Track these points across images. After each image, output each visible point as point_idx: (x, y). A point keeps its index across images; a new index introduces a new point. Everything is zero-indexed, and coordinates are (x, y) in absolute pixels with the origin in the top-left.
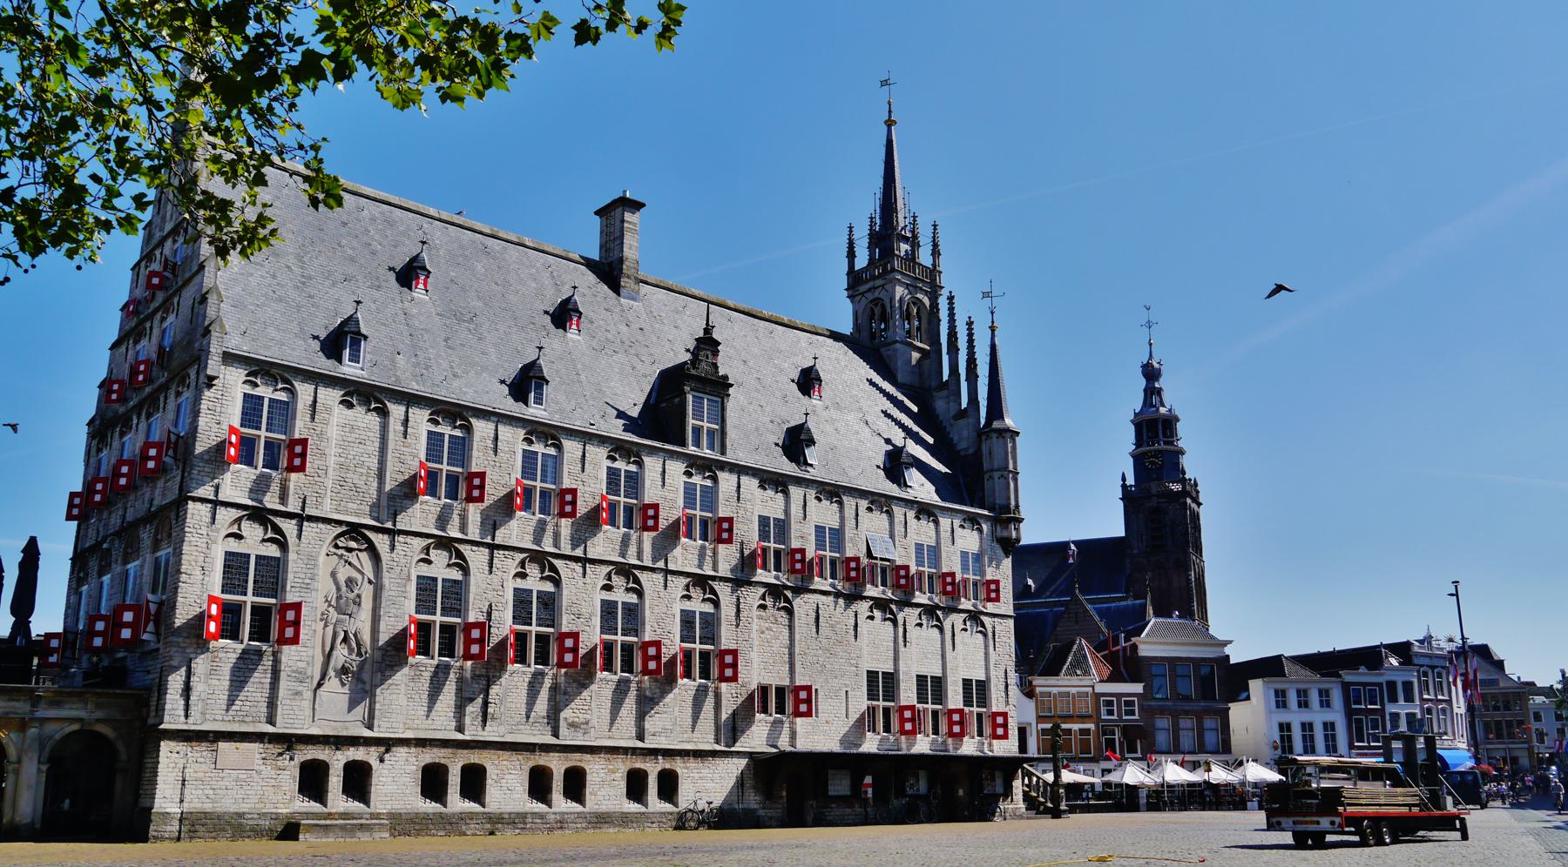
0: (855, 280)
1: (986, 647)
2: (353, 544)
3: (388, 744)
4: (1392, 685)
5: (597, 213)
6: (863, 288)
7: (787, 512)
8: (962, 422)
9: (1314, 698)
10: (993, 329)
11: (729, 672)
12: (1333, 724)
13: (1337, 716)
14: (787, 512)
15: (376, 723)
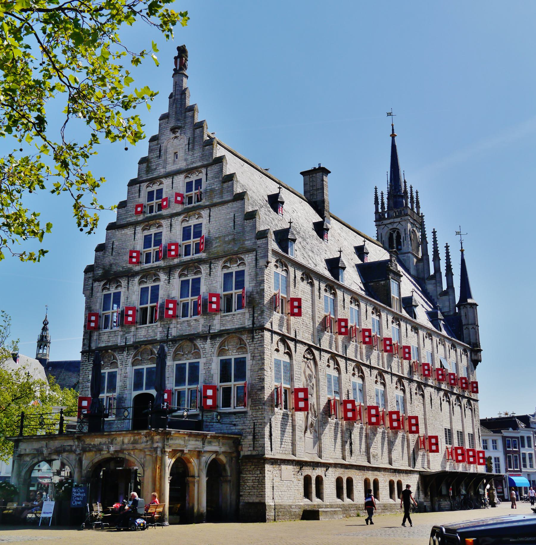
0: (379, 218)
1: (472, 416)
2: (309, 356)
3: (327, 466)
4: (522, 438)
5: (302, 173)
6: (385, 222)
7: (418, 344)
8: (445, 298)
9: (490, 445)
10: (462, 251)
11: (414, 428)
12: (498, 458)
13: (499, 454)
14: (418, 344)
15: (323, 454)
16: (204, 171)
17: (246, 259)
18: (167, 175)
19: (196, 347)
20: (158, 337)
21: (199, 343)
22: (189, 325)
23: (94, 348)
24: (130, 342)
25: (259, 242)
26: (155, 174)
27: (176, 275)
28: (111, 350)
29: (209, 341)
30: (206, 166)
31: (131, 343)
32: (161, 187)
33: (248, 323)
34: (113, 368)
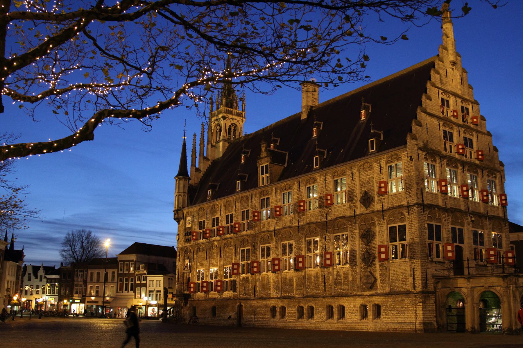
16: (471, 104)
24: (449, 207)
25: (501, 168)
30: (472, 103)
32: (448, 99)
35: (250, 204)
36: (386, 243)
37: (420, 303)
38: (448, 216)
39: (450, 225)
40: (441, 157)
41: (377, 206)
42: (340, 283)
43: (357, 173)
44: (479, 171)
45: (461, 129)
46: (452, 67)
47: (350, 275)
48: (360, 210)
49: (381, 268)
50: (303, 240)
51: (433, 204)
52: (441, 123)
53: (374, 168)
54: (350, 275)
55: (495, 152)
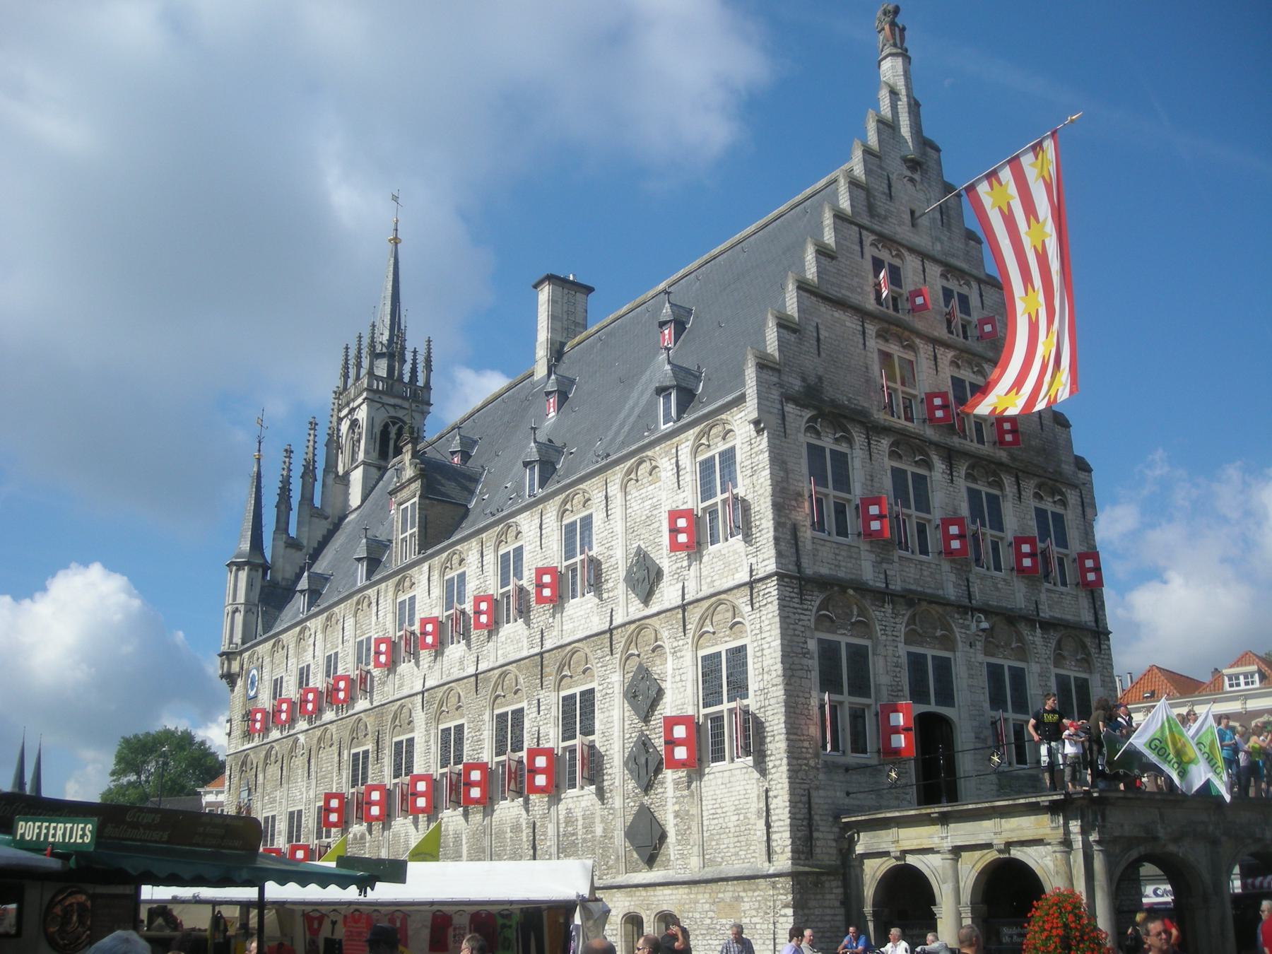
16: (974, 285)
17: (1069, 496)
18: (912, 250)
19: (1020, 639)
20: (951, 591)
21: (1025, 631)
22: (998, 589)
23: (809, 572)
24: (896, 586)
25: (1082, 475)
26: (886, 230)
27: (963, 473)
28: (855, 589)
29: (1039, 631)
30: (979, 281)
31: (898, 588)
33: (1087, 617)
34: (857, 636)
35: (374, 618)
36: (690, 711)
37: (786, 906)
38: (895, 615)
39: (901, 645)
40: (867, 429)
41: (668, 595)
42: (574, 844)
43: (620, 495)
44: (1008, 481)
45: (940, 351)
46: (909, 173)
47: (598, 820)
48: (627, 607)
49: (678, 794)
50: (487, 717)
51: (841, 574)
52: (871, 329)
53: (663, 474)
54: (598, 820)
55: (1058, 429)
